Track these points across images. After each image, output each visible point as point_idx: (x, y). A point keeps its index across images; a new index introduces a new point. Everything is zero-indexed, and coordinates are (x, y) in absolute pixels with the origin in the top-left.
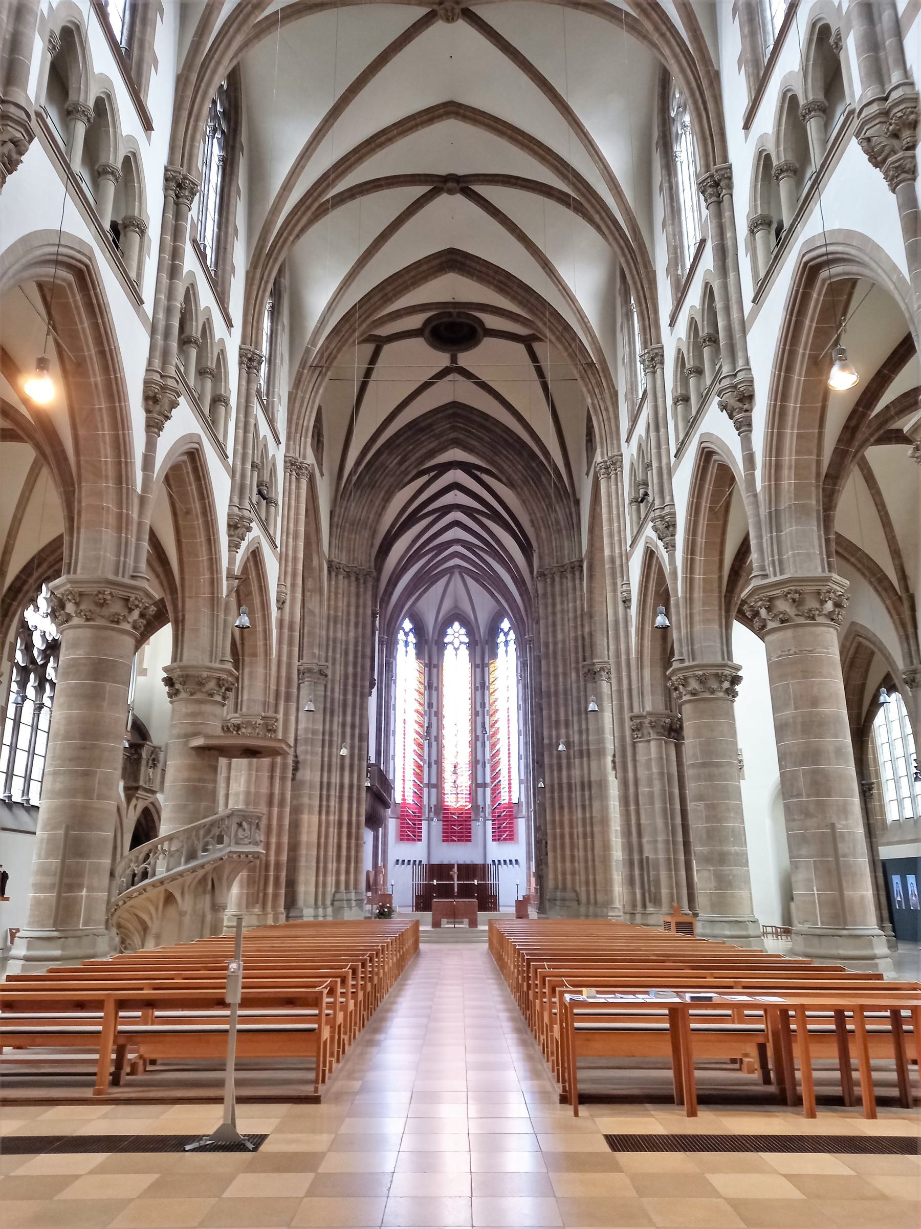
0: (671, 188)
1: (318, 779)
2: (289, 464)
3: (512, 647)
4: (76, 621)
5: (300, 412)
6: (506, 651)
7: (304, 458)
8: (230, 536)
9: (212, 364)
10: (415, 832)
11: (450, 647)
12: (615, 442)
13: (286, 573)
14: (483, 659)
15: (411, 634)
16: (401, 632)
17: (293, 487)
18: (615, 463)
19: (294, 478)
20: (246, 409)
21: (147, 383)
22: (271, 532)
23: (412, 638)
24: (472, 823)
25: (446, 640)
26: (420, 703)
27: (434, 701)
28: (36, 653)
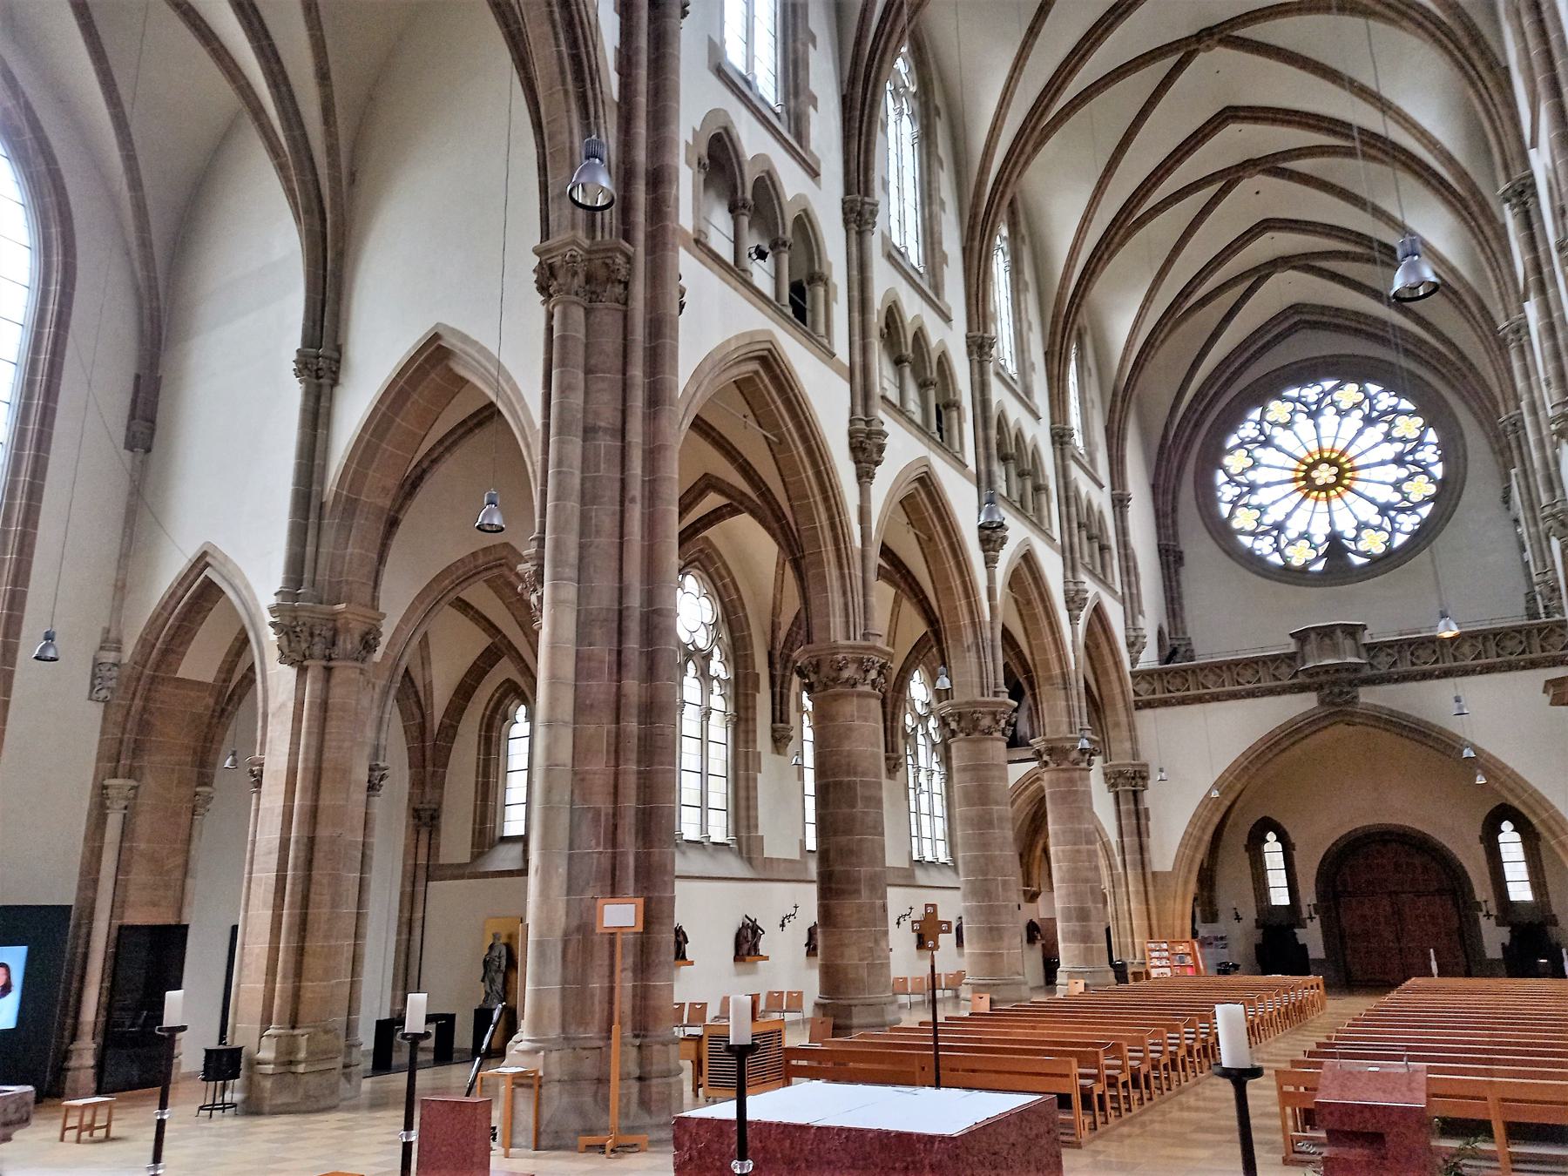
4: (962, 735)
9: (1028, 466)
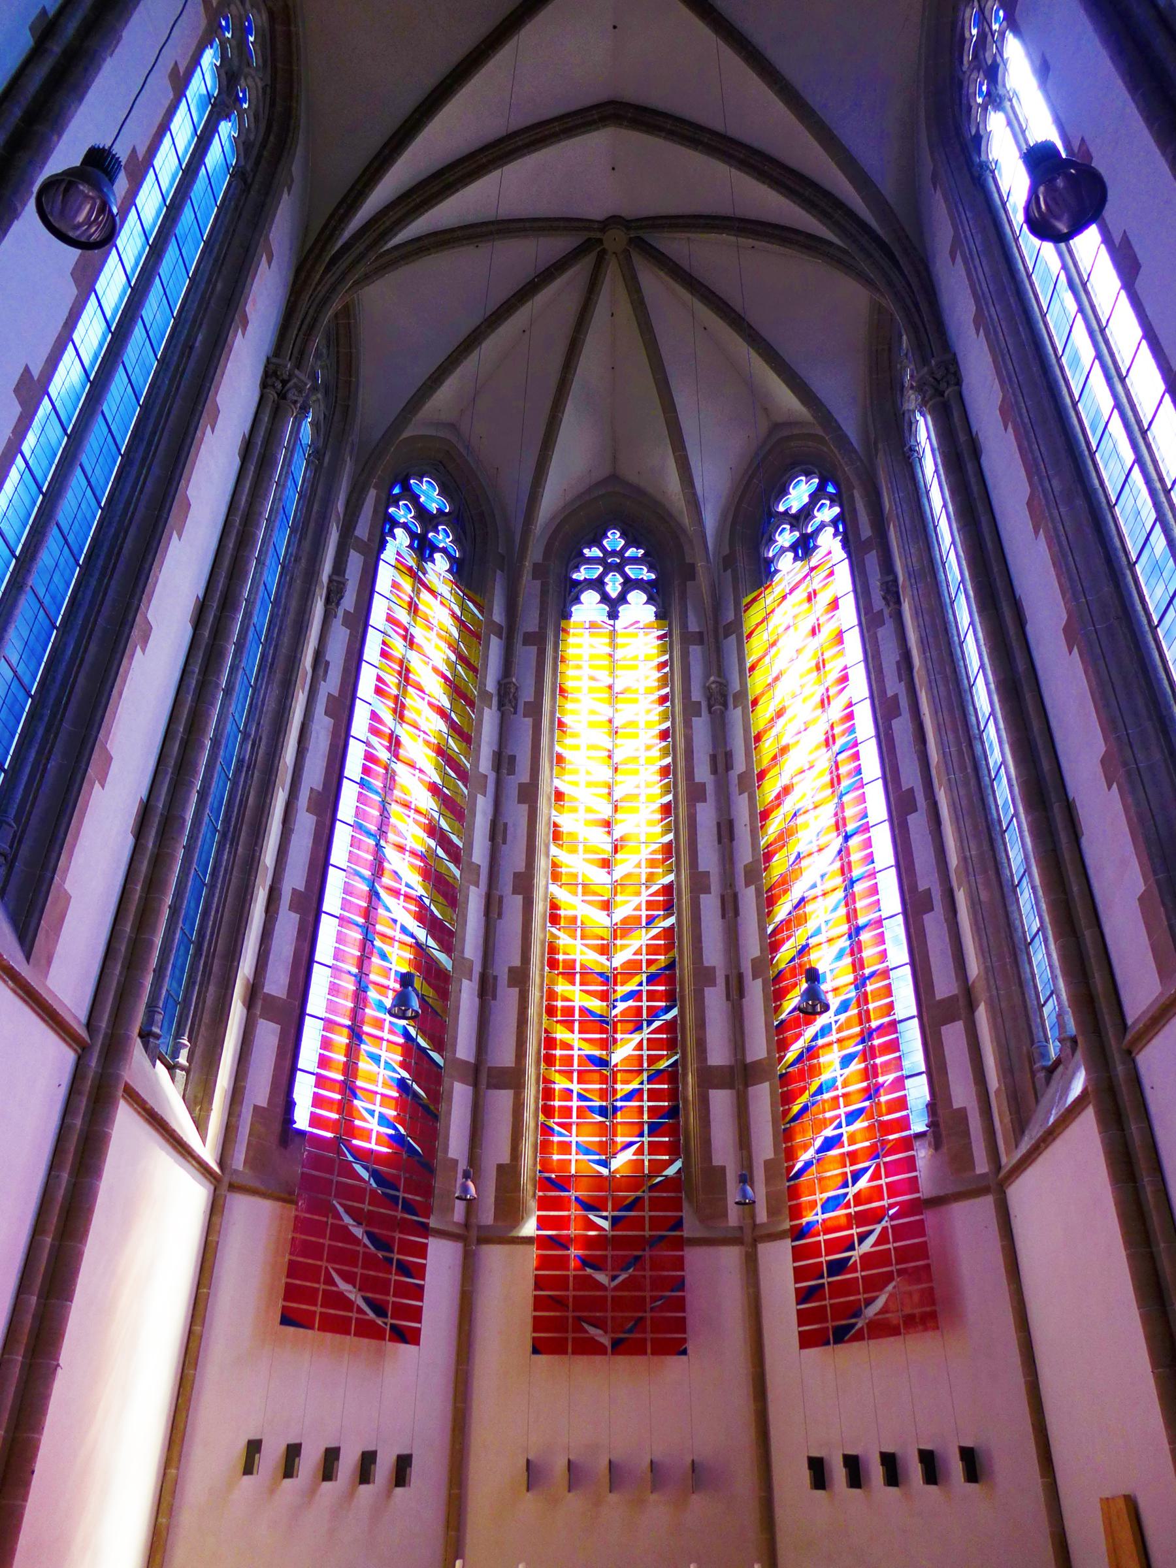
3: (829, 543)
10: (382, 1286)
11: (590, 597)
23: (442, 538)
24: (692, 1255)
26: (452, 726)
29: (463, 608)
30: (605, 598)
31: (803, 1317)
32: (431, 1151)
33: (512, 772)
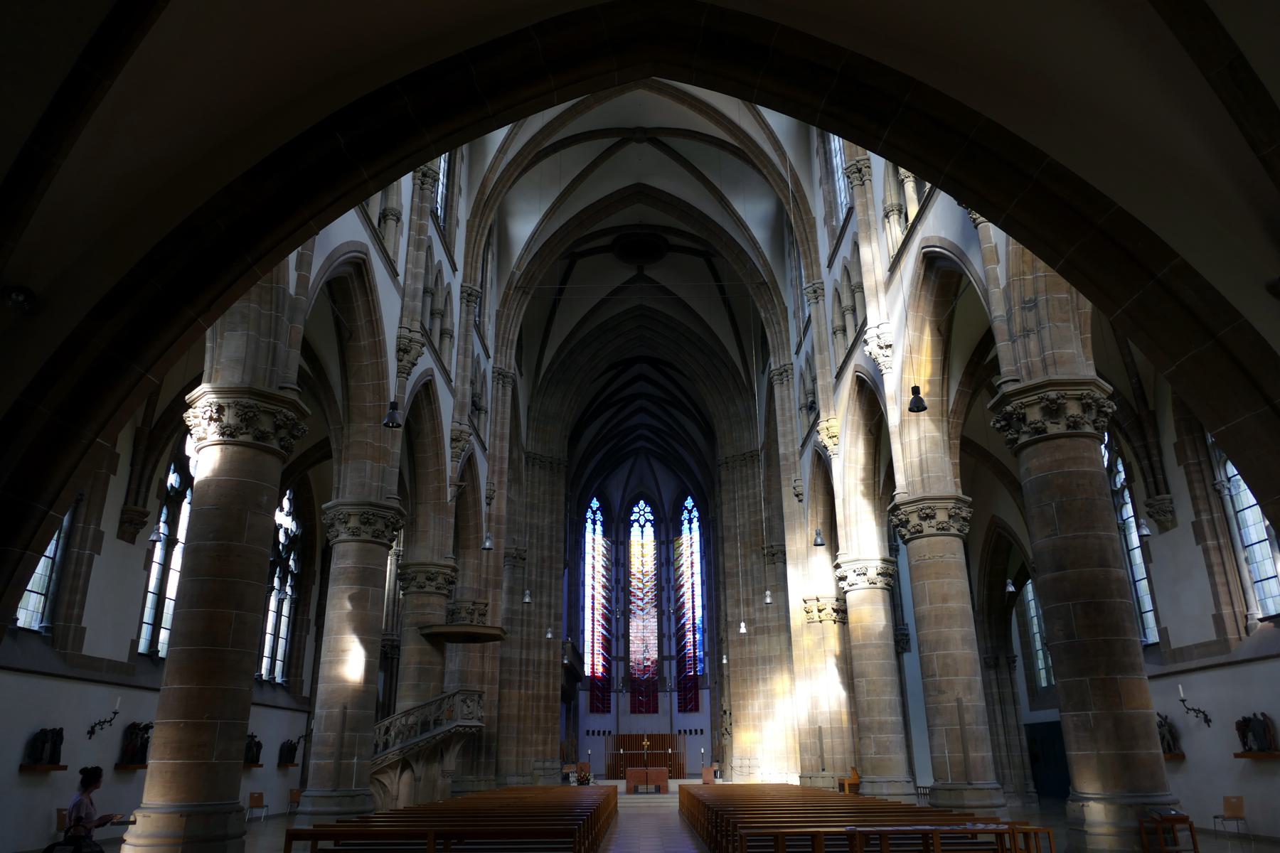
0: (825, 153)
1: (517, 656)
2: (496, 374)
3: (696, 525)
5: (505, 327)
6: (690, 529)
7: (510, 368)
8: (452, 448)
11: (636, 525)
12: (786, 352)
13: (493, 472)
14: (667, 536)
15: (598, 512)
16: (589, 510)
17: (500, 394)
18: (785, 371)
19: (500, 386)
20: (466, 337)
21: (399, 337)
22: (482, 436)
23: (599, 516)
25: (632, 518)
27: (621, 577)
28: (281, 547)
29: (606, 544)
30: (640, 526)
31: (679, 707)
32: (610, 677)
33: (619, 583)
